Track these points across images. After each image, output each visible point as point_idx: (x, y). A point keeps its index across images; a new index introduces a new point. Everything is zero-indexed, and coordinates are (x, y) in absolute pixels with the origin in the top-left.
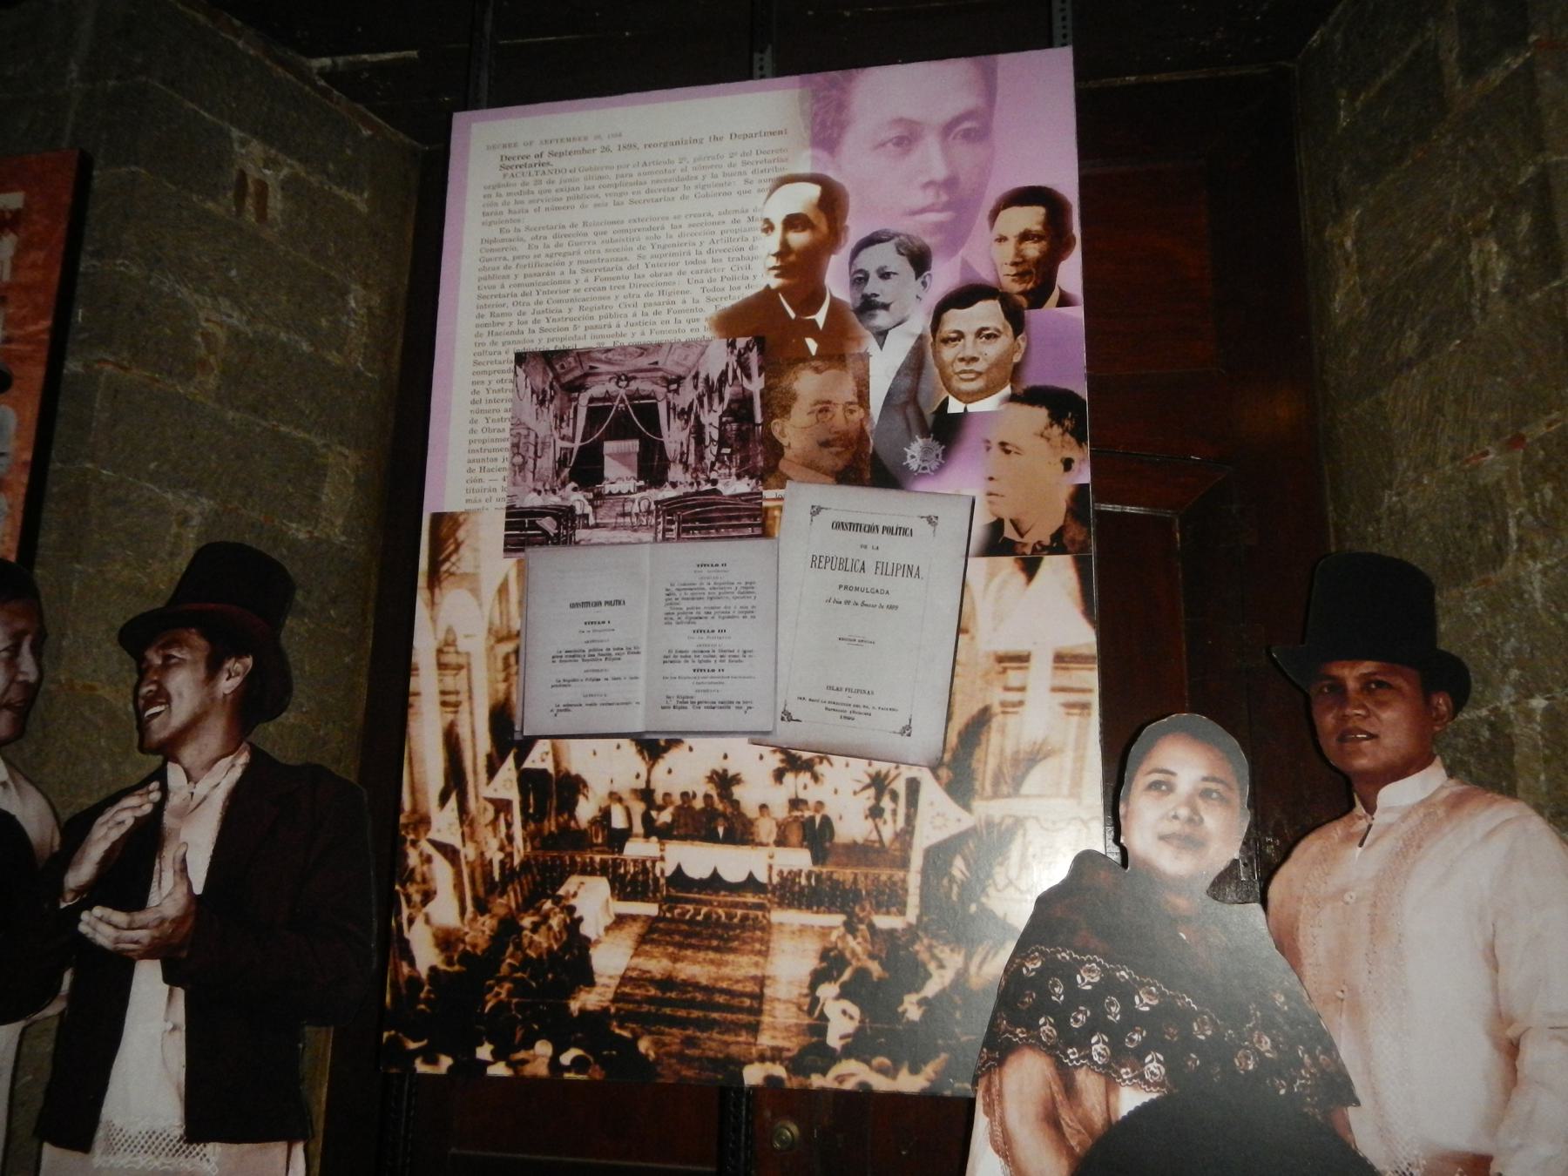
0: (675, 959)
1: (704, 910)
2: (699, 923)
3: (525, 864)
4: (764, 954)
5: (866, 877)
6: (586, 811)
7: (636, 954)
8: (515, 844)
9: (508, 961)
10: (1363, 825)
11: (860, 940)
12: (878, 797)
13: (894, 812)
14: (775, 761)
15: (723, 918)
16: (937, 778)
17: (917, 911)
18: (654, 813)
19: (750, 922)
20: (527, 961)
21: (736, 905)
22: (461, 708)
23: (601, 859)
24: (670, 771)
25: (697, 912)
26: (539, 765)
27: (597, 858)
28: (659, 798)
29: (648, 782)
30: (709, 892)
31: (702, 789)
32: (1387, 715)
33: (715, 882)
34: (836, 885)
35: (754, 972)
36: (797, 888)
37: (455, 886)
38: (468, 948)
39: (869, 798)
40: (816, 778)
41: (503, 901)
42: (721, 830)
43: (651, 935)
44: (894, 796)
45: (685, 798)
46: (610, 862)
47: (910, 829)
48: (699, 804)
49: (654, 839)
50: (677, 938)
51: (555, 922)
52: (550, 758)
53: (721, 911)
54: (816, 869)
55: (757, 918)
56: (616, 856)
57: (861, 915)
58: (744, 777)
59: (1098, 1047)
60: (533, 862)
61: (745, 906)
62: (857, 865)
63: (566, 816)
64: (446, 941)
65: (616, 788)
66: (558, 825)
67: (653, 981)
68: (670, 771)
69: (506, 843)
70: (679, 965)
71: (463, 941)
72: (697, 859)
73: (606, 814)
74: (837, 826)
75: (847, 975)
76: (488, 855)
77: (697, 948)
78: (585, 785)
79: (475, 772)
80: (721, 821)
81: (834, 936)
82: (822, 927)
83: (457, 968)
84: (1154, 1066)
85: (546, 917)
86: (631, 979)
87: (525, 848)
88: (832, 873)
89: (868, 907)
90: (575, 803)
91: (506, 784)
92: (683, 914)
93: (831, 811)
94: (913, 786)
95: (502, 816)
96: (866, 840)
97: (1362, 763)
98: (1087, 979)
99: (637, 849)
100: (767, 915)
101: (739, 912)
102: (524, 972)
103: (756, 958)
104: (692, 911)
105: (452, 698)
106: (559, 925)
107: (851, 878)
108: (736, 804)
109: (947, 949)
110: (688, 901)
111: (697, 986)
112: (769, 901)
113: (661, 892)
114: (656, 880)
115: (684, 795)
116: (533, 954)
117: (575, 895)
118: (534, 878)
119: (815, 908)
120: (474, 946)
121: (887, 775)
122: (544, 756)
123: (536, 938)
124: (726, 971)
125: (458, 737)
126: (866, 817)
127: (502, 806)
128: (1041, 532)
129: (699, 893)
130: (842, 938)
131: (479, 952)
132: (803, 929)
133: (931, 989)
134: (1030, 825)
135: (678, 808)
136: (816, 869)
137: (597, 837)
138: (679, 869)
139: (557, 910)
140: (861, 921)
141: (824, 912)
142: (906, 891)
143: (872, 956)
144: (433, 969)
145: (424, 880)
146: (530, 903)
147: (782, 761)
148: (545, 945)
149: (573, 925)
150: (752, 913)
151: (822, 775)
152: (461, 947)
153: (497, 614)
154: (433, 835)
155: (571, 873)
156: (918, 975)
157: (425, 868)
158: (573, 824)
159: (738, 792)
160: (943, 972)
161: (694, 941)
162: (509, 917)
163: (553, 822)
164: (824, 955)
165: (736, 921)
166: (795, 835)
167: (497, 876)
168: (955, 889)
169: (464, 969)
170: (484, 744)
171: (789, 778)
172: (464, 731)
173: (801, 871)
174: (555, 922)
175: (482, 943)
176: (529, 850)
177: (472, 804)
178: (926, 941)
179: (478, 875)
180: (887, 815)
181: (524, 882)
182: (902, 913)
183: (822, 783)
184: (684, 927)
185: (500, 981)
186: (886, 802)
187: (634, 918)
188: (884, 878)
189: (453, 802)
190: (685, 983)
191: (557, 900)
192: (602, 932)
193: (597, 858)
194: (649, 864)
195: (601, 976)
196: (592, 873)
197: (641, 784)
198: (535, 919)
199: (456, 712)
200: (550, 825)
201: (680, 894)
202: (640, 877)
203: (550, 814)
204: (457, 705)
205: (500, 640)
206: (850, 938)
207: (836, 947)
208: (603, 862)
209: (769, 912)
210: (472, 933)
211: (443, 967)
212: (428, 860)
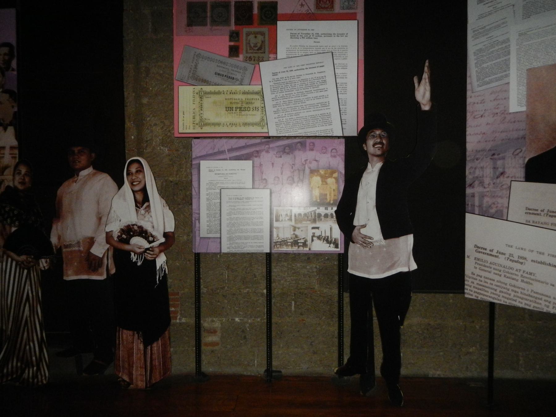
10: (76, 179)
32: (83, 158)
59: (9, 221)
84: (17, 223)
97: (77, 167)
98: (7, 209)
128: (7, 122)
134: (6, 181)
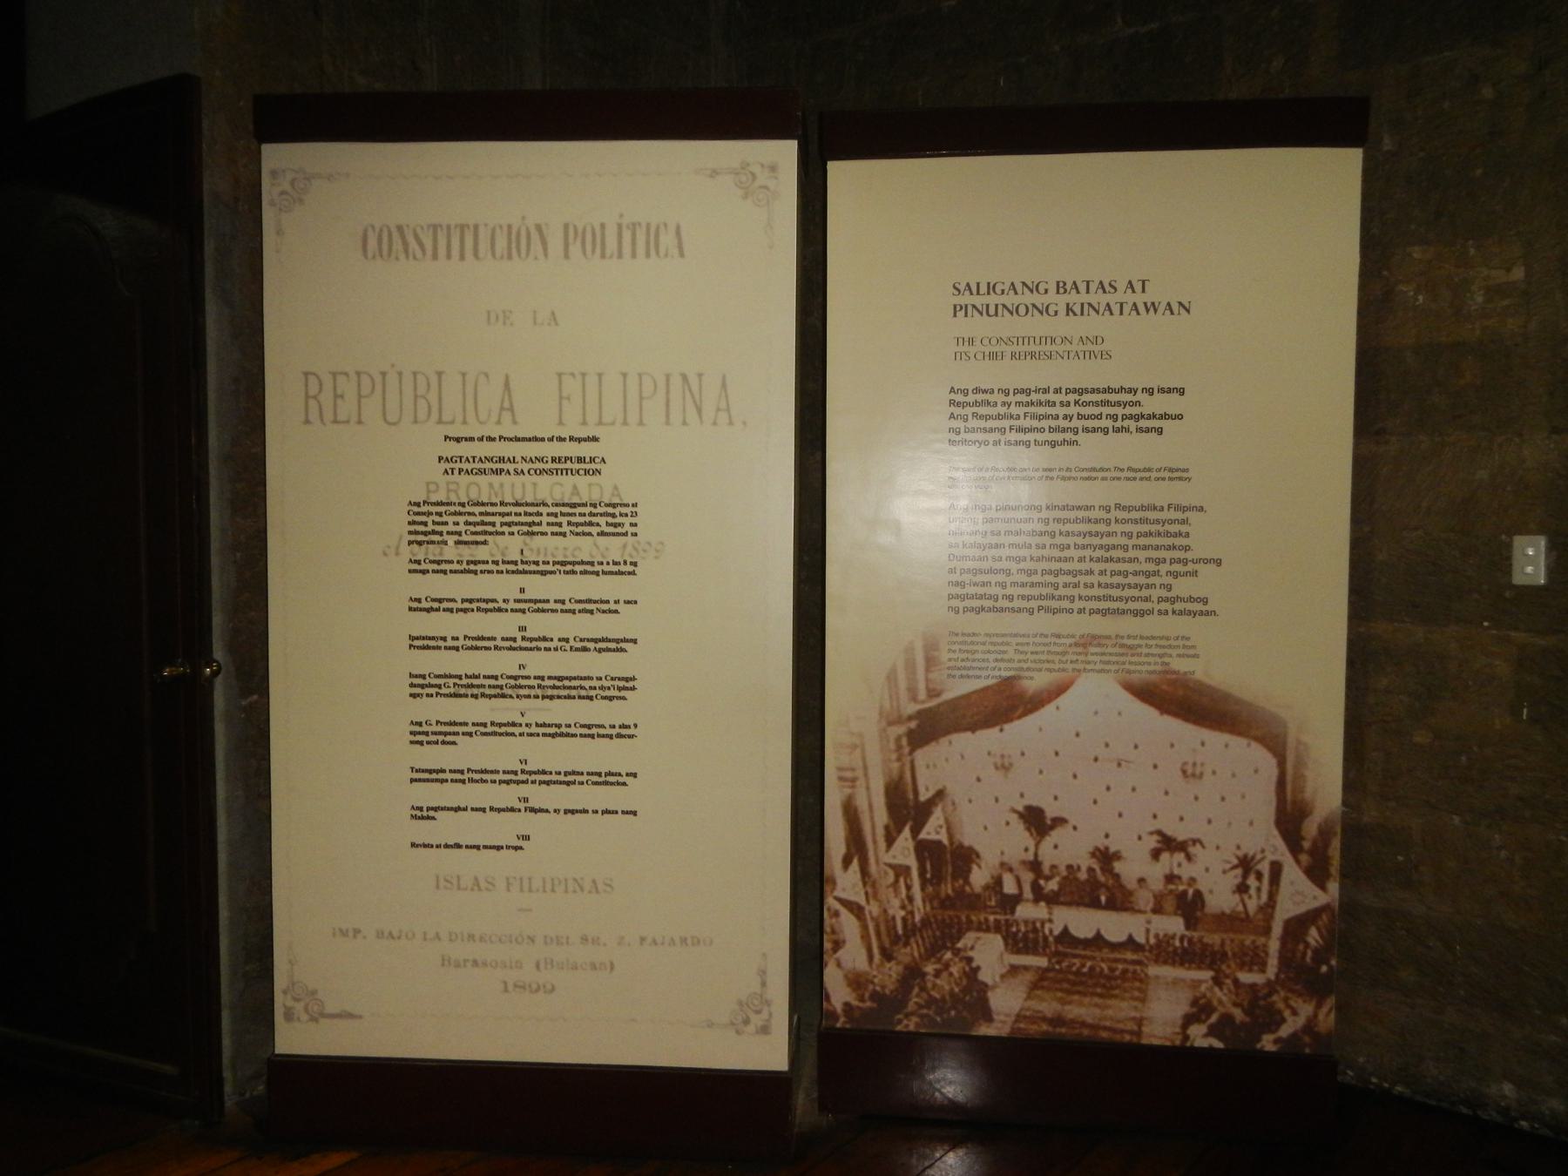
0: (1063, 1002)
1: (1089, 964)
2: (1084, 974)
3: (926, 922)
4: (1143, 1000)
5: (1232, 941)
6: (979, 878)
7: (1029, 997)
8: (915, 903)
9: (916, 1000)
11: (1225, 991)
12: (1245, 876)
13: (1259, 890)
14: (1152, 842)
15: (1106, 971)
16: (1298, 862)
17: (1275, 970)
18: (1042, 882)
19: (1130, 975)
20: (931, 1002)
21: (1116, 961)
22: (858, 783)
23: (996, 920)
24: (1056, 847)
25: (1083, 966)
26: (933, 837)
27: (991, 918)
28: (1046, 870)
29: (1036, 855)
30: (1093, 949)
33: (1098, 941)
34: (1205, 946)
35: (1133, 1014)
36: (1171, 949)
37: (862, 937)
38: (878, 988)
39: (1236, 877)
40: (1189, 858)
41: (908, 950)
42: (1103, 899)
44: (1259, 876)
45: (1071, 870)
46: (1003, 922)
47: (1272, 903)
48: (1083, 876)
49: (1043, 904)
50: (1065, 986)
51: (955, 970)
52: (944, 830)
53: (1104, 966)
55: (1135, 972)
56: (1008, 917)
57: (1228, 972)
58: (1124, 854)
60: (932, 920)
61: (1125, 961)
62: (1226, 931)
63: (961, 882)
64: (856, 982)
65: (1006, 859)
66: (953, 890)
67: (1044, 1019)
68: (1056, 847)
69: (906, 902)
70: (1067, 1008)
71: (872, 983)
72: (1083, 922)
73: (998, 882)
74: (1208, 898)
75: (1214, 1018)
76: (891, 912)
77: (1084, 994)
78: (978, 856)
79: (875, 842)
80: (1103, 890)
81: (1203, 988)
82: (1193, 981)
83: (868, 1004)
85: (947, 966)
86: (1025, 1017)
87: (924, 907)
88: (1203, 937)
89: (1233, 966)
90: (969, 871)
91: (904, 851)
92: (1070, 966)
93: (1202, 886)
94: (1276, 869)
95: (902, 880)
96: (1233, 911)
100: (1146, 970)
101: (1120, 966)
102: (929, 1008)
103: (1135, 1003)
104: (1078, 965)
105: (849, 774)
106: (958, 972)
108: (1117, 877)
109: (1300, 1001)
110: (1075, 956)
111: (1083, 1024)
112: (1147, 958)
113: (1049, 947)
114: (1045, 938)
115: (1069, 867)
117: (972, 948)
118: (934, 932)
119: (1187, 965)
120: (883, 987)
121: (1253, 858)
122: (939, 829)
123: (938, 982)
124: (1110, 1012)
125: (856, 810)
126: (1234, 892)
127: (901, 871)
129: (1084, 949)
130: (1211, 989)
131: (887, 992)
132: (1176, 982)
133: (1285, 1031)
135: (1065, 878)
136: (1187, 933)
137: (990, 900)
138: (1066, 930)
139: (957, 960)
140: (1227, 977)
141: (1195, 969)
142: (1267, 954)
143: (1235, 1005)
144: (847, 1004)
145: (833, 932)
146: (933, 952)
147: (1159, 842)
148: (947, 988)
149: (972, 973)
150: (1131, 968)
151: (1195, 855)
152: (871, 987)
153: (886, 697)
155: (969, 929)
156: (1276, 1021)
157: (834, 920)
158: (967, 889)
159: (1118, 866)
160: (1297, 1019)
161: (1080, 988)
162: (913, 964)
163: (949, 886)
164: (1195, 1003)
165: (1117, 973)
166: (1169, 904)
167: (900, 932)
168: (1309, 953)
169: (875, 1005)
170: (882, 817)
171: (1165, 856)
172: (861, 802)
173: (1175, 935)
174: (955, 970)
175: (891, 986)
176: (928, 908)
177: (873, 868)
178: (1282, 994)
179: (883, 928)
180: (1252, 891)
181: (925, 935)
182: (1263, 971)
183: (1196, 862)
184: (1071, 977)
185: (907, 1016)
186: (1252, 881)
187: (1026, 968)
188: (1248, 943)
189: (855, 865)
190: (1073, 1021)
191: (957, 952)
192: (998, 979)
193: (991, 918)
194: (1038, 925)
195: (998, 1014)
196: (988, 930)
197: (1030, 856)
198: (938, 966)
199: (853, 787)
200: (946, 890)
201: (1069, 950)
202: (1031, 936)
203: (946, 880)
204: (854, 780)
205: (890, 724)
206: (1216, 989)
207: (1204, 996)
209: (1147, 966)
210: (880, 977)
211: (855, 1003)
212: (836, 914)
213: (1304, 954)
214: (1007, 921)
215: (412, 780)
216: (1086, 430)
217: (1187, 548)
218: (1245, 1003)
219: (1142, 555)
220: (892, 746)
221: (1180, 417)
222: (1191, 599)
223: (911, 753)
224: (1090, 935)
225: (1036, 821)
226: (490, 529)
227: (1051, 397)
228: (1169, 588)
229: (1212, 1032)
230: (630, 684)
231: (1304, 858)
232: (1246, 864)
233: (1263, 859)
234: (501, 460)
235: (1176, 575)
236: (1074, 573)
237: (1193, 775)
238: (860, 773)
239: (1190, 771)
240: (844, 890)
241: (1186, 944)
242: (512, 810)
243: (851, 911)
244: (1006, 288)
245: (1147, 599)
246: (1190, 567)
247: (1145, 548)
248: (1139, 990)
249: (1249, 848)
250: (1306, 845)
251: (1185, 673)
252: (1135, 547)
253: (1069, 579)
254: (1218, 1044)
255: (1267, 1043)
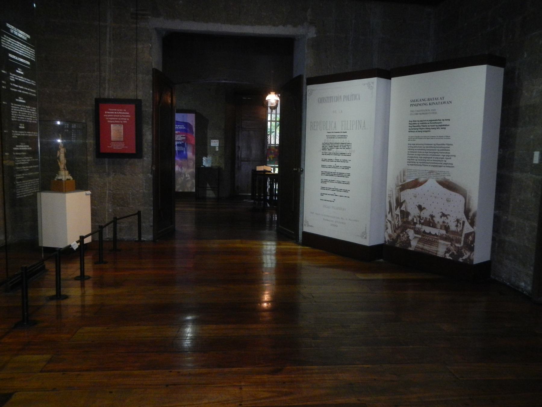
1: (428, 238)
3: (401, 225)
4: (437, 247)
5: (455, 237)
6: (410, 218)
9: (399, 241)
12: (458, 223)
13: (460, 226)
14: (440, 214)
15: (431, 240)
16: (468, 221)
18: (421, 220)
20: (401, 242)
21: (433, 238)
25: (427, 238)
26: (403, 209)
27: (412, 226)
28: (422, 218)
29: (420, 215)
31: (428, 217)
33: (430, 234)
34: (449, 237)
40: (447, 218)
41: (398, 231)
43: (420, 240)
44: (460, 224)
49: (421, 225)
51: (405, 236)
52: (405, 208)
54: (446, 234)
55: (436, 241)
68: (423, 213)
72: (428, 229)
73: (413, 219)
74: (450, 227)
75: (450, 253)
78: (410, 214)
79: (394, 209)
81: (449, 246)
82: (447, 244)
85: (404, 235)
86: (417, 247)
90: (409, 217)
91: (398, 212)
94: (464, 222)
99: (418, 226)
101: (434, 239)
103: (436, 247)
105: (390, 196)
107: (452, 237)
108: (434, 221)
109: (467, 252)
110: (426, 236)
114: (421, 232)
115: (426, 218)
116: (402, 240)
117: (408, 232)
123: (403, 238)
124: (432, 249)
126: (455, 226)
127: (397, 215)
130: (450, 246)
132: (444, 244)
133: (464, 258)
136: (446, 234)
142: (461, 240)
143: (455, 251)
144: (388, 240)
146: (402, 232)
147: (442, 214)
149: (408, 237)
150: (436, 240)
154: (387, 218)
159: (434, 219)
160: (466, 255)
161: (427, 243)
164: (447, 249)
166: (443, 228)
167: (397, 227)
171: (443, 217)
172: (392, 202)
175: (395, 238)
178: (464, 250)
179: (394, 226)
180: (459, 227)
184: (425, 240)
185: (398, 244)
186: (459, 225)
187: (417, 237)
188: (458, 238)
189: (390, 213)
191: (406, 232)
196: (411, 229)
197: (419, 215)
198: (403, 235)
208: (413, 227)
211: (389, 240)
213: (469, 242)
214: (414, 227)
215: (321, 189)
216: (432, 129)
217: (449, 153)
218: (457, 251)
219: (441, 154)
220: (397, 191)
221: (449, 125)
222: (450, 164)
223: (400, 192)
224: (429, 232)
225: (420, 208)
226: (332, 147)
227: (426, 122)
228: (445, 161)
229: (450, 256)
230: (349, 175)
231: (469, 221)
232: (458, 221)
233: (461, 220)
234: (334, 136)
235: (447, 159)
236: (428, 158)
237: (449, 201)
238: (392, 196)
239: (448, 200)
240: (388, 218)
241: (446, 236)
242: (333, 195)
243: (389, 222)
244: (419, 100)
245: (441, 164)
246: (450, 157)
247: (442, 153)
248: (437, 245)
249: (459, 217)
250: (470, 218)
251: (448, 179)
252: (440, 152)
253: (428, 159)
254: (451, 258)
255: (461, 260)
